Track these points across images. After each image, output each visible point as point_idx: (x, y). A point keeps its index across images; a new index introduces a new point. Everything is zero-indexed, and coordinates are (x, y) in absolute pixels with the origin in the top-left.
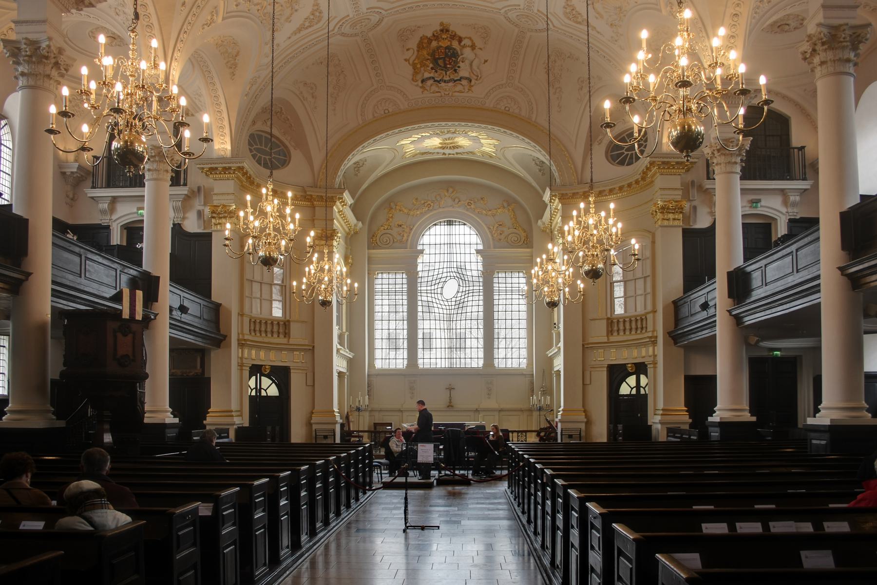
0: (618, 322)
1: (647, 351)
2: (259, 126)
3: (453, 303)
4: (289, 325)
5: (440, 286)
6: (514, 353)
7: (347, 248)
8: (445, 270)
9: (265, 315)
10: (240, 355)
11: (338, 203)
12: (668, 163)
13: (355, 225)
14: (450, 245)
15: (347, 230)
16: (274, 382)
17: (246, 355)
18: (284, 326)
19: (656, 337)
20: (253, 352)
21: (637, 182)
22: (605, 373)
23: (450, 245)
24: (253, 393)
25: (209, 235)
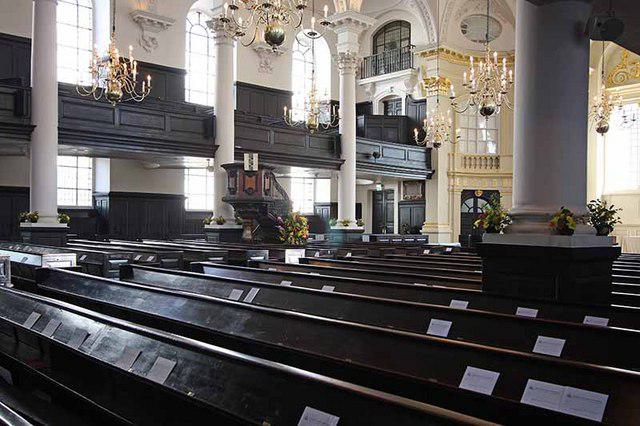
9: (480, 152)
18: (496, 161)
24: (472, 211)
25: (425, 101)
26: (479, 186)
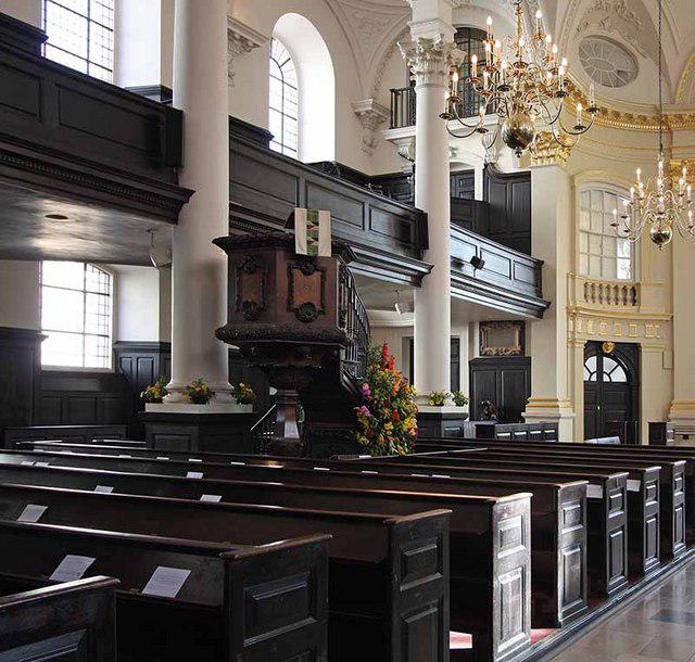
2: (594, 29)
4: (639, 290)
9: (607, 277)
10: (571, 329)
16: (620, 364)
17: (579, 329)
18: (632, 293)
20: (591, 324)
24: (594, 378)
25: (528, 175)
26: (610, 334)
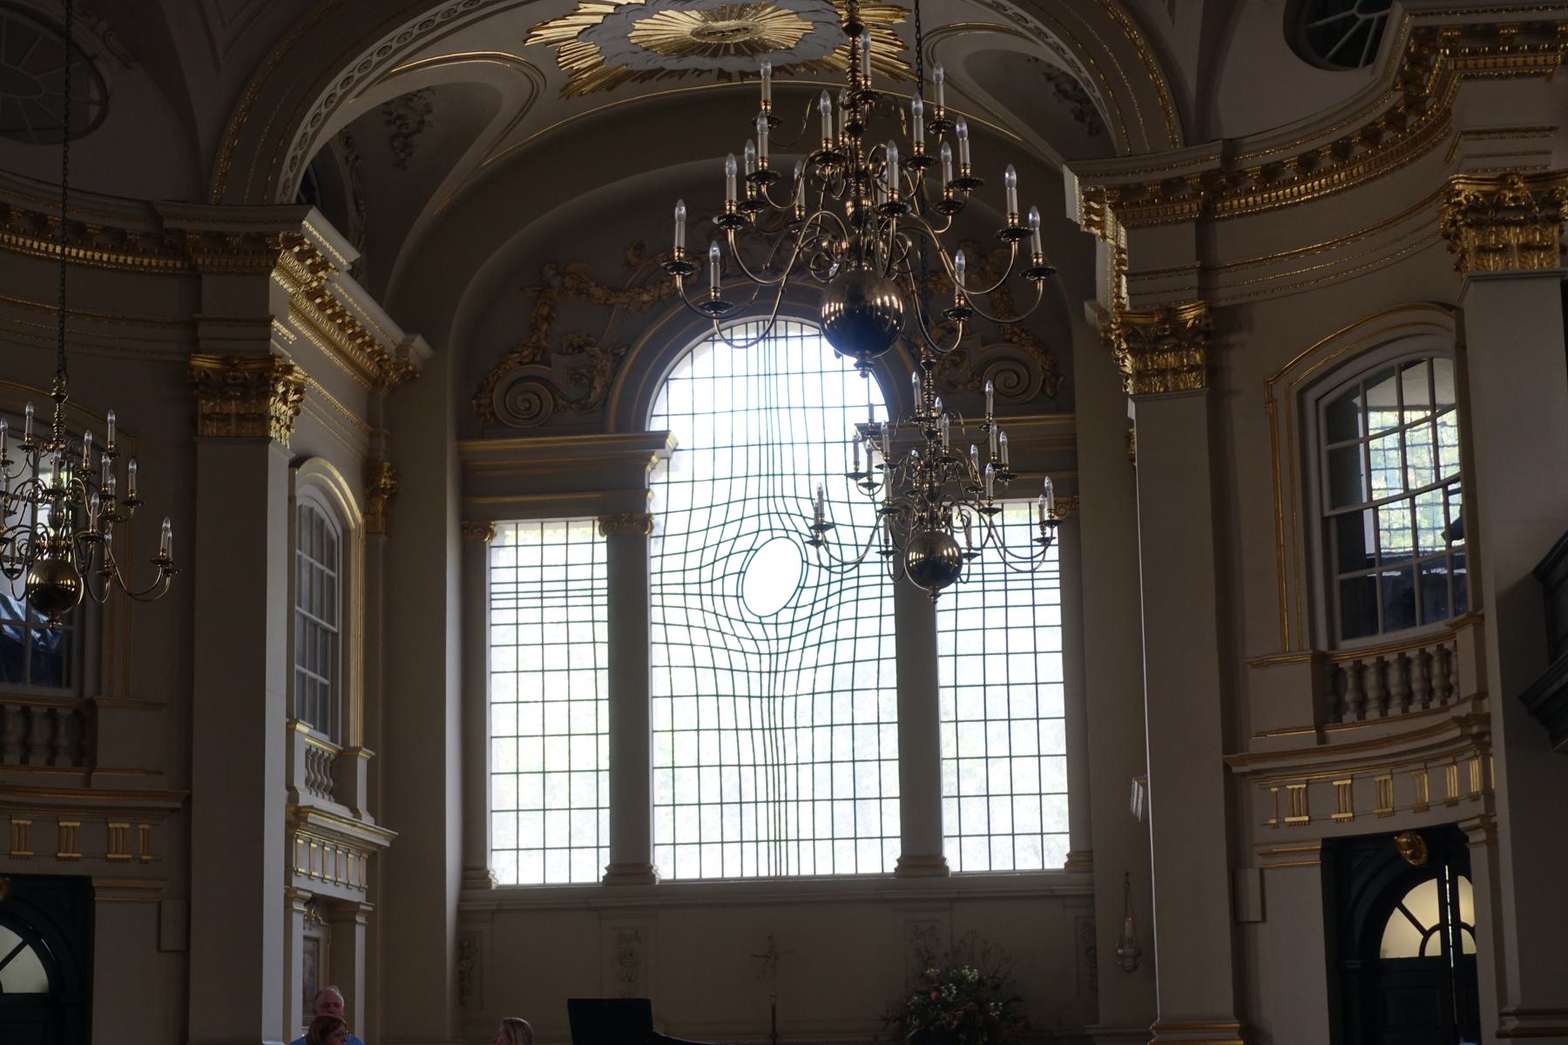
0: (1360, 670)
1: (1464, 780)
3: (784, 631)
5: (735, 564)
6: (1014, 814)
7: (371, 435)
8: (751, 508)
11: (288, 259)
12: (1490, 32)
13: (402, 349)
14: (764, 419)
15: (370, 366)
19: (1486, 719)
21: (1394, 120)
22: (1315, 875)
23: (764, 419)
